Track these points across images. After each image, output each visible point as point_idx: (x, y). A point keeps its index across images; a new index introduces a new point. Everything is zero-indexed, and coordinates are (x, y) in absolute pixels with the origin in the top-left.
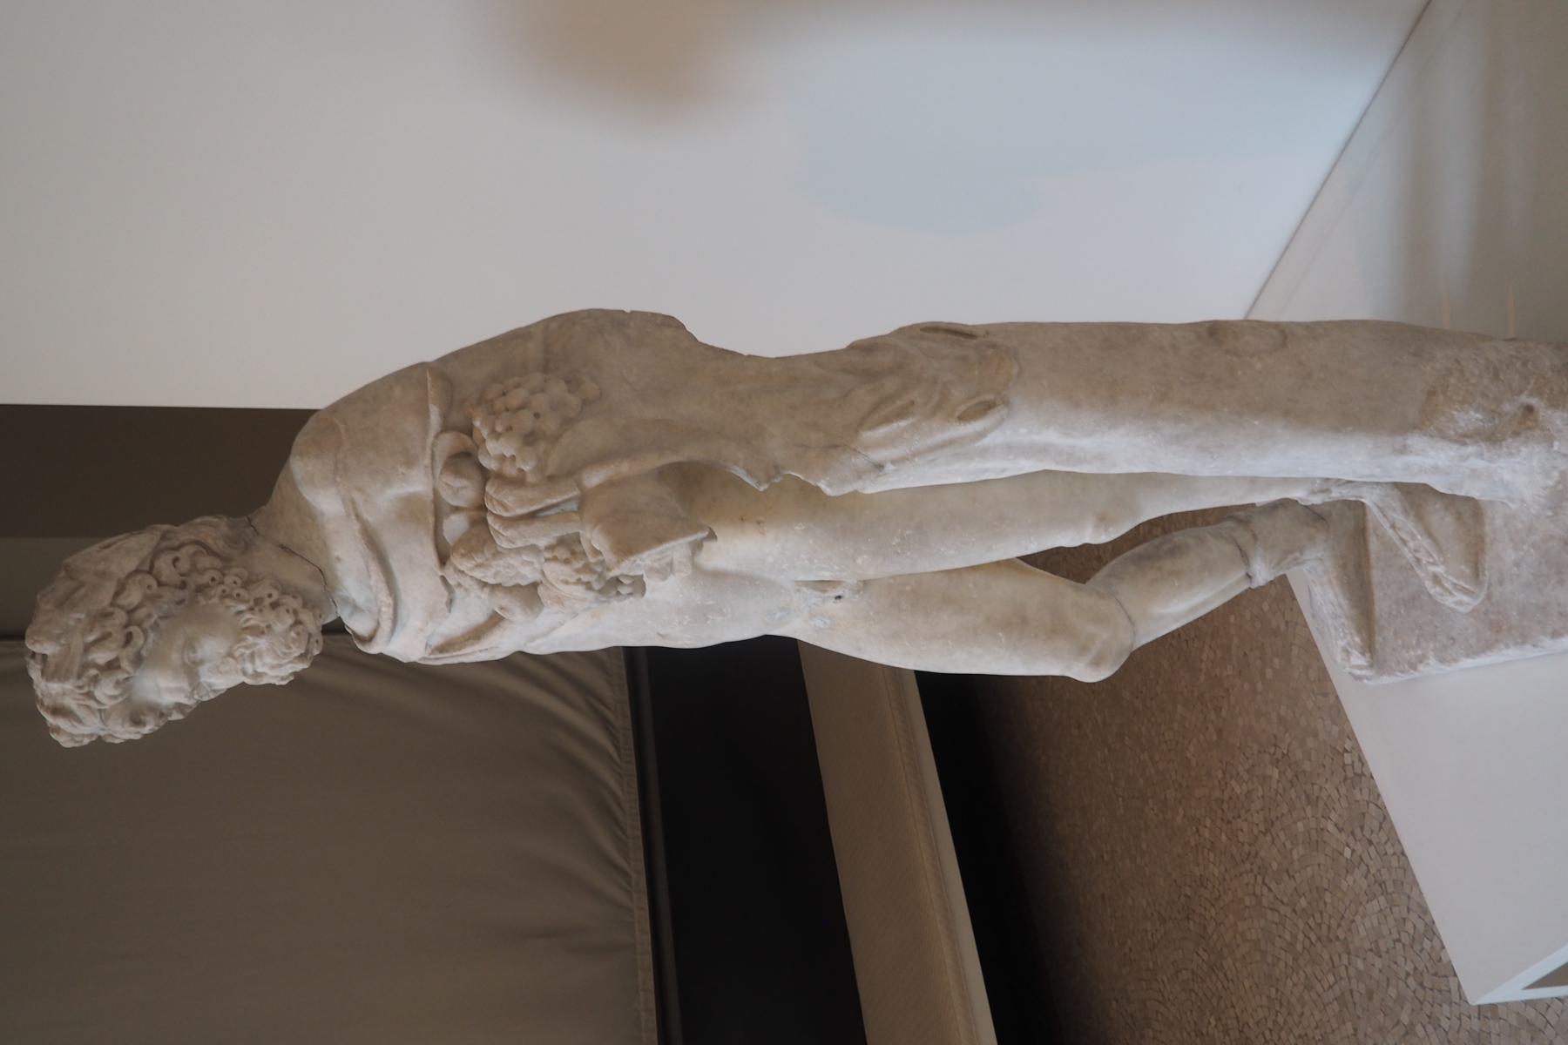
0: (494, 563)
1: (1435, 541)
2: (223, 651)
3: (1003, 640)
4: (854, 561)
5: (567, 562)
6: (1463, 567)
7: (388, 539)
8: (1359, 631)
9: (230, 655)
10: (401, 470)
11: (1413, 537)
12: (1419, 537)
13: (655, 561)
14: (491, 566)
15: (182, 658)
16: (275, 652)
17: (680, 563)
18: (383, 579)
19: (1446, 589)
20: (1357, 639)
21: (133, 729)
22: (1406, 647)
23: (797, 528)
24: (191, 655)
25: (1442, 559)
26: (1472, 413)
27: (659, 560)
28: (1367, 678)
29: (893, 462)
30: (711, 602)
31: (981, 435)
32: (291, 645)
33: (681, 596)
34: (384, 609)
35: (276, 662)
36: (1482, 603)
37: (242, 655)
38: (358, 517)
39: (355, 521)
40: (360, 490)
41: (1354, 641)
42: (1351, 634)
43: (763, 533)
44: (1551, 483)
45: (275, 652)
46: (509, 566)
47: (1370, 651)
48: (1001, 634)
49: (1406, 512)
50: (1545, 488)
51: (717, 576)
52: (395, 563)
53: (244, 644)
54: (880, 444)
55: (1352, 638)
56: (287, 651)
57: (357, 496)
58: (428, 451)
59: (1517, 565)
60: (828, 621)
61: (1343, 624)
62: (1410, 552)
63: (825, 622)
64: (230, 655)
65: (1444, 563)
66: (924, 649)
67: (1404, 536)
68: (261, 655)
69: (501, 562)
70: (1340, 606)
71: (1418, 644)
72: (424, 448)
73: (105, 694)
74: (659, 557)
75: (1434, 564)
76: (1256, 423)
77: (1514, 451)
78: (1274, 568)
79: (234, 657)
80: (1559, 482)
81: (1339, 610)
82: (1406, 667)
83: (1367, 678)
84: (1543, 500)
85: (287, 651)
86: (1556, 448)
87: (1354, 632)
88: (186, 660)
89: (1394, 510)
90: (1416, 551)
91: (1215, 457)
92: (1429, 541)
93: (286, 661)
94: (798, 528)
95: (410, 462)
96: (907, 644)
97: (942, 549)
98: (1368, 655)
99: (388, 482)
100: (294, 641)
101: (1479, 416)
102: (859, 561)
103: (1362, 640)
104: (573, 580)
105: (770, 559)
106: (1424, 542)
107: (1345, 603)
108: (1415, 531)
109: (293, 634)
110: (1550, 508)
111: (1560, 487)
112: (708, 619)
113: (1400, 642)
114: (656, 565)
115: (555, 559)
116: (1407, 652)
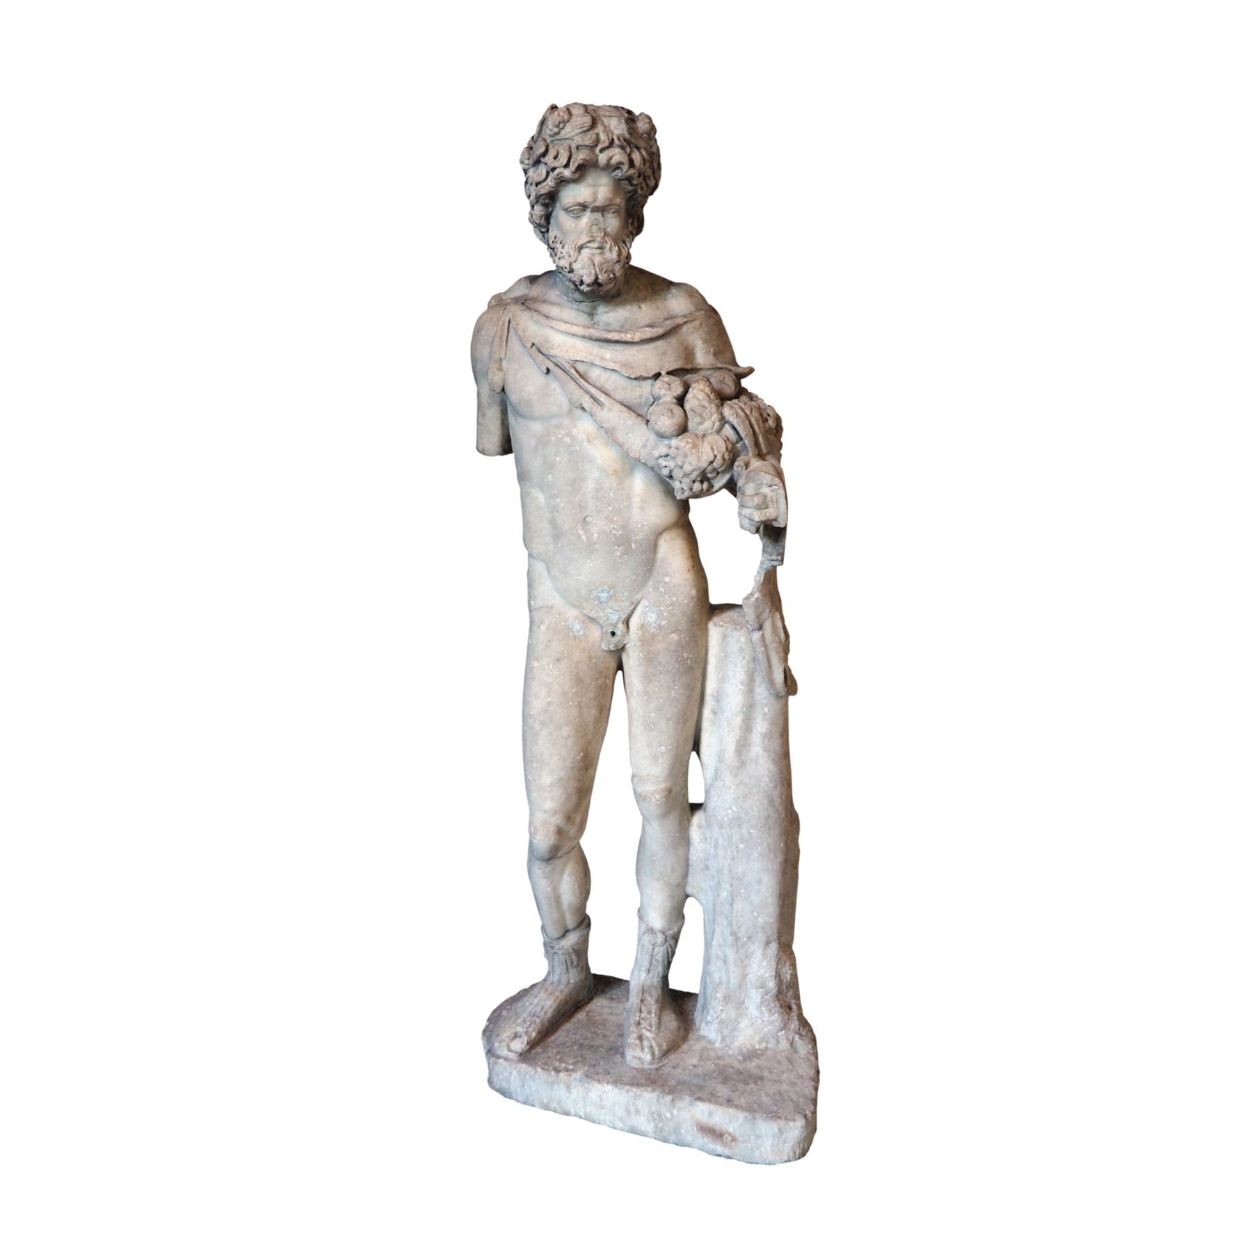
0: (714, 406)
1: (660, 1023)
2: (609, 229)
3: (579, 757)
4: (673, 632)
5: (727, 448)
6: (664, 1044)
7: (673, 340)
8: (539, 1033)
9: (606, 234)
10: (712, 350)
11: (649, 1013)
12: (653, 1015)
13: (772, 498)
14: (710, 403)
15: (615, 205)
16: (605, 263)
17: (766, 513)
18: (654, 336)
19: (642, 1045)
20: (534, 1034)
21: (576, 164)
22: (561, 1060)
23: (694, 590)
24: (613, 210)
25: (656, 1032)
26: (790, 972)
27: (772, 501)
28: (506, 1059)
29: (763, 635)
30: (633, 546)
31: (771, 682)
32: (606, 274)
33: (639, 526)
34: (629, 336)
35: (596, 263)
36: (650, 1069)
37: (606, 242)
38: (685, 323)
39: (684, 321)
40: (701, 324)
41: (531, 1034)
42: (534, 1029)
43: (689, 571)
44: (757, 1047)
45: (605, 263)
46: (712, 415)
47: (530, 1048)
48: (582, 754)
49: (657, 1001)
50: (753, 1046)
51: (654, 547)
52: (660, 343)
53: (613, 244)
54: (774, 626)
55: (533, 1031)
56: (603, 271)
57: (697, 323)
58: (724, 366)
59: (695, 1066)
60: (581, 633)
61: (535, 1022)
62: (639, 1017)
63: (579, 631)
64: (606, 234)
65: (656, 1034)
66: (571, 703)
67: (643, 1009)
68: (602, 254)
69: (714, 410)
70: (546, 1013)
71: (573, 1064)
72: (724, 363)
73: (616, 154)
74: (774, 500)
75: (649, 1030)
76: (782, 844)
77: (773, 1011)
78: (573, 949)
79: (604, 236)
80: (761, 1050)
81: (542, 1013)
82: (551, 1068)
83: (506, 1059)
84: (745, 1050)
85: (603, 271)
86: (780, 1034)
87: (536, 1030)
88: (612, 207)
89: (651, 996)
90: (643, 1019)
91: (763, 829)
92: (657, 1020)
93: (598, 270)
94: (694, 592)
95: (716, 354)
96: (574, 691)
97: (677, 687)
98: (528, 1047)
99: (705, 341)
100: (609, 276)
101: (788, 978)
102: (673, 635)
103: (535, 1038)
104: (716, 453)
105: (667, 579)
106: (654, 1020)
107: (549, 1015)
108: (653, 1011)
109: (612, 276)
110: (744, 1056)
111: (759, 1052)
112: (619, 546)
113: (558, 1057)
114: (769, 499)
115: (725, 441)
116: (560, 1063)
